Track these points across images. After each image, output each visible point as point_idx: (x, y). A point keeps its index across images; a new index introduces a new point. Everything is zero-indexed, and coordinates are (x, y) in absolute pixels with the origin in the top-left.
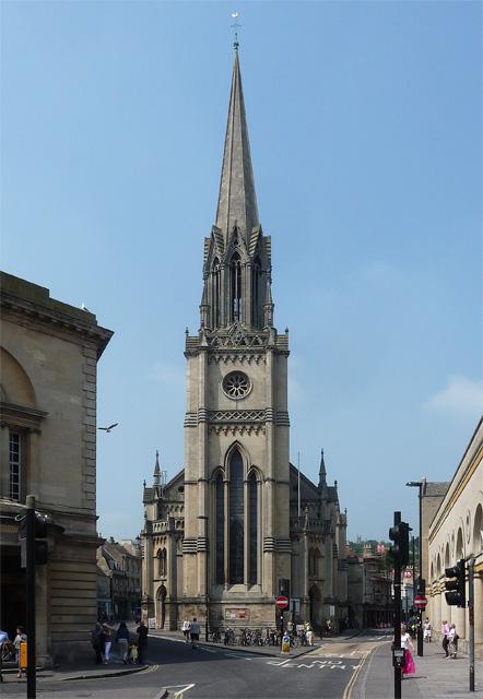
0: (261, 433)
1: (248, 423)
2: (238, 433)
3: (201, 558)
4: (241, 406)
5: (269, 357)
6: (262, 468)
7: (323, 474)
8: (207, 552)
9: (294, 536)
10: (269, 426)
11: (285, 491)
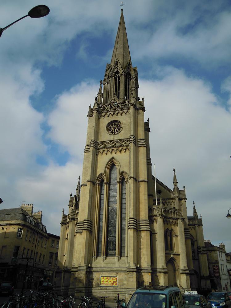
0: (127, 151)
1: (120, 147)
2: (113, 152)
3: (85, 234)
4: (117, 137)
5: (132, 109)
6: (128, 172)
7: (175, 183)
8: (90, 231)
9: (151, 219)
10: (132, 145)
11: (143, 188)
